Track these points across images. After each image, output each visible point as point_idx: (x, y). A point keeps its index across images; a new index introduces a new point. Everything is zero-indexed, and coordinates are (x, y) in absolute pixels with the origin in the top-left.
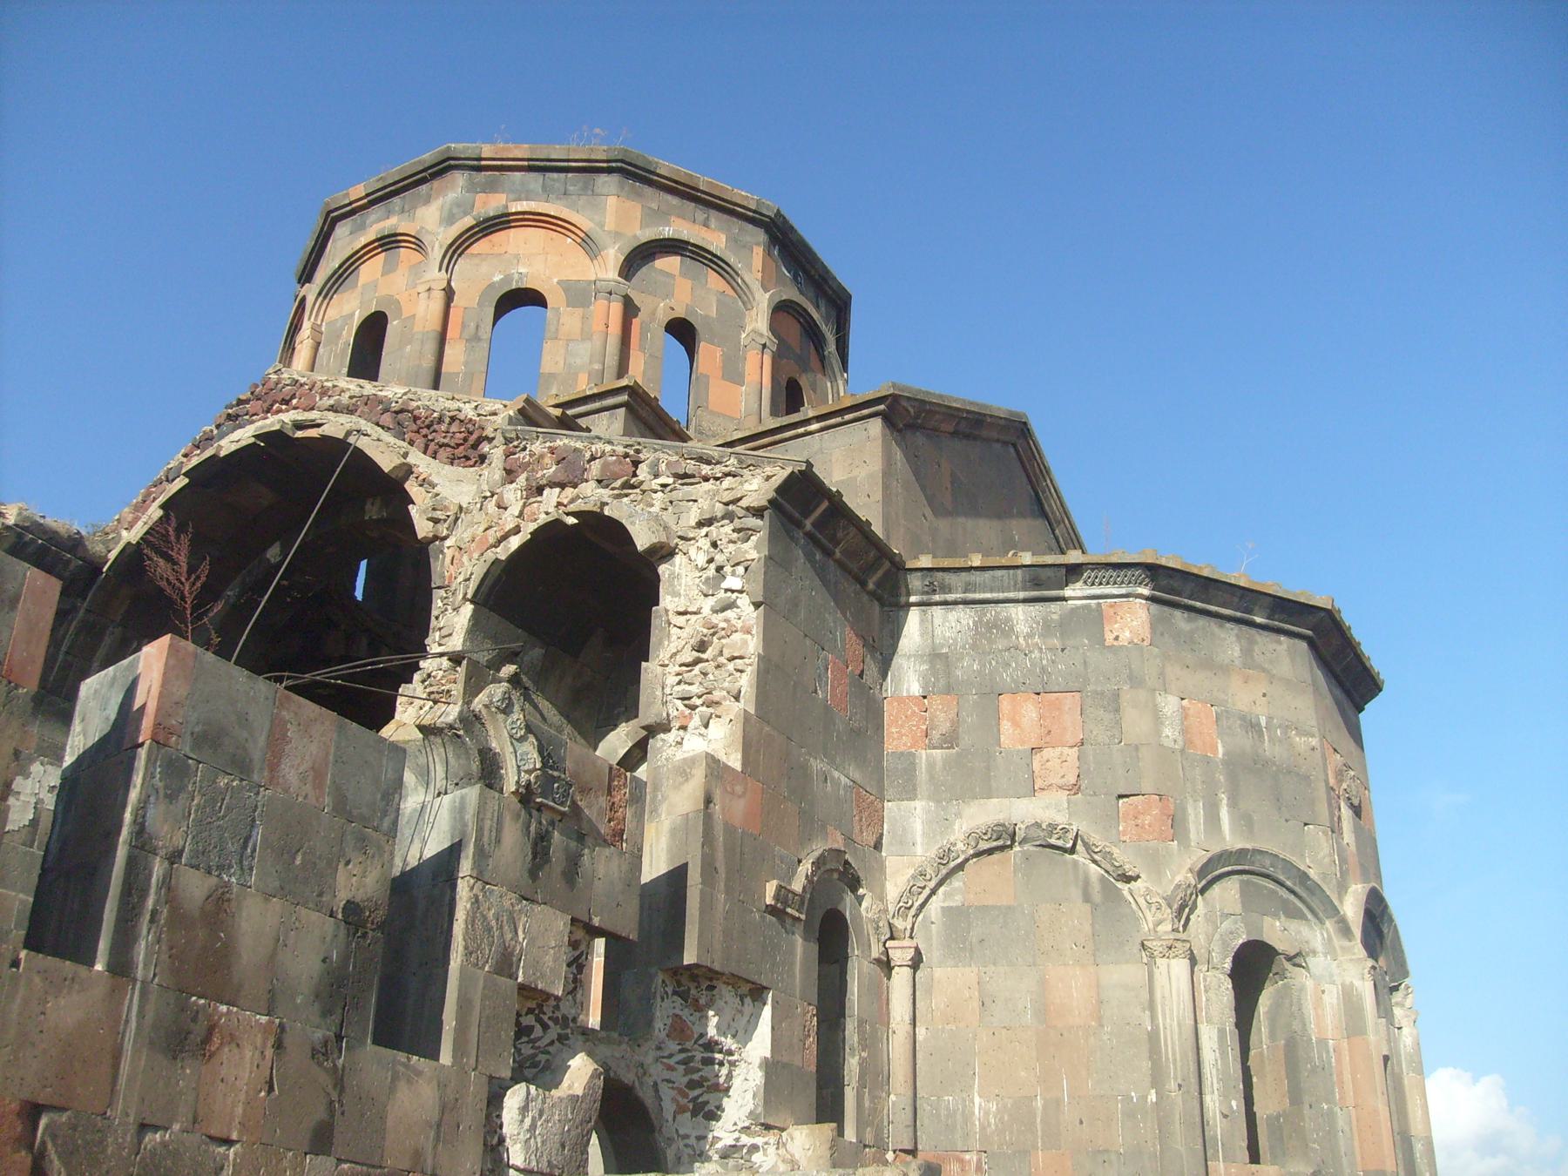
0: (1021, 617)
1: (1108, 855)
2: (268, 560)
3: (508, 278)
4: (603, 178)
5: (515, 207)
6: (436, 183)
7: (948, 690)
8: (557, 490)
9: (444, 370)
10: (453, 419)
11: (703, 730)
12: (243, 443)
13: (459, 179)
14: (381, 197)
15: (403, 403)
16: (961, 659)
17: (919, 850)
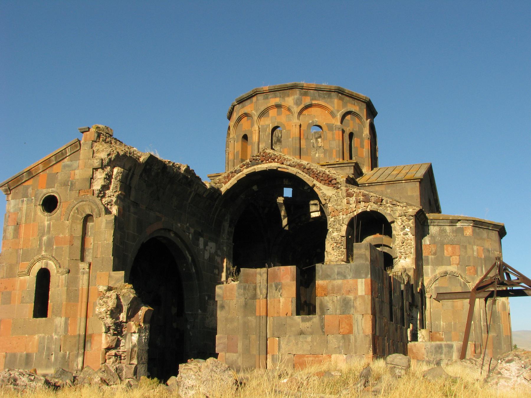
0: (448, 229)
1: (465, 278)
2: (254, 190)
3: (313, 122)
4: (333, 94)
5: (314, 102)
6: (290, 91)
7: (434, 243)
8: (364, 203)
9: (301, 147)
10: (323, 173)
11: (405, 259)
12: (263, 169)
13: (297, 91)
14: (274, 91)
15: (309, 167)
16: (437, 237)
17: (430, 275)
